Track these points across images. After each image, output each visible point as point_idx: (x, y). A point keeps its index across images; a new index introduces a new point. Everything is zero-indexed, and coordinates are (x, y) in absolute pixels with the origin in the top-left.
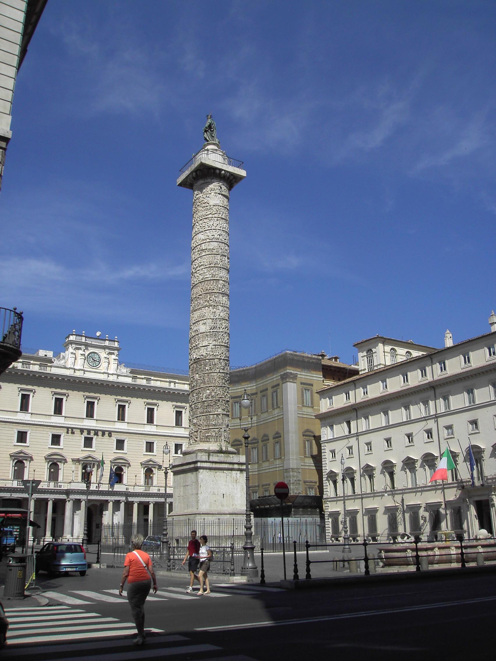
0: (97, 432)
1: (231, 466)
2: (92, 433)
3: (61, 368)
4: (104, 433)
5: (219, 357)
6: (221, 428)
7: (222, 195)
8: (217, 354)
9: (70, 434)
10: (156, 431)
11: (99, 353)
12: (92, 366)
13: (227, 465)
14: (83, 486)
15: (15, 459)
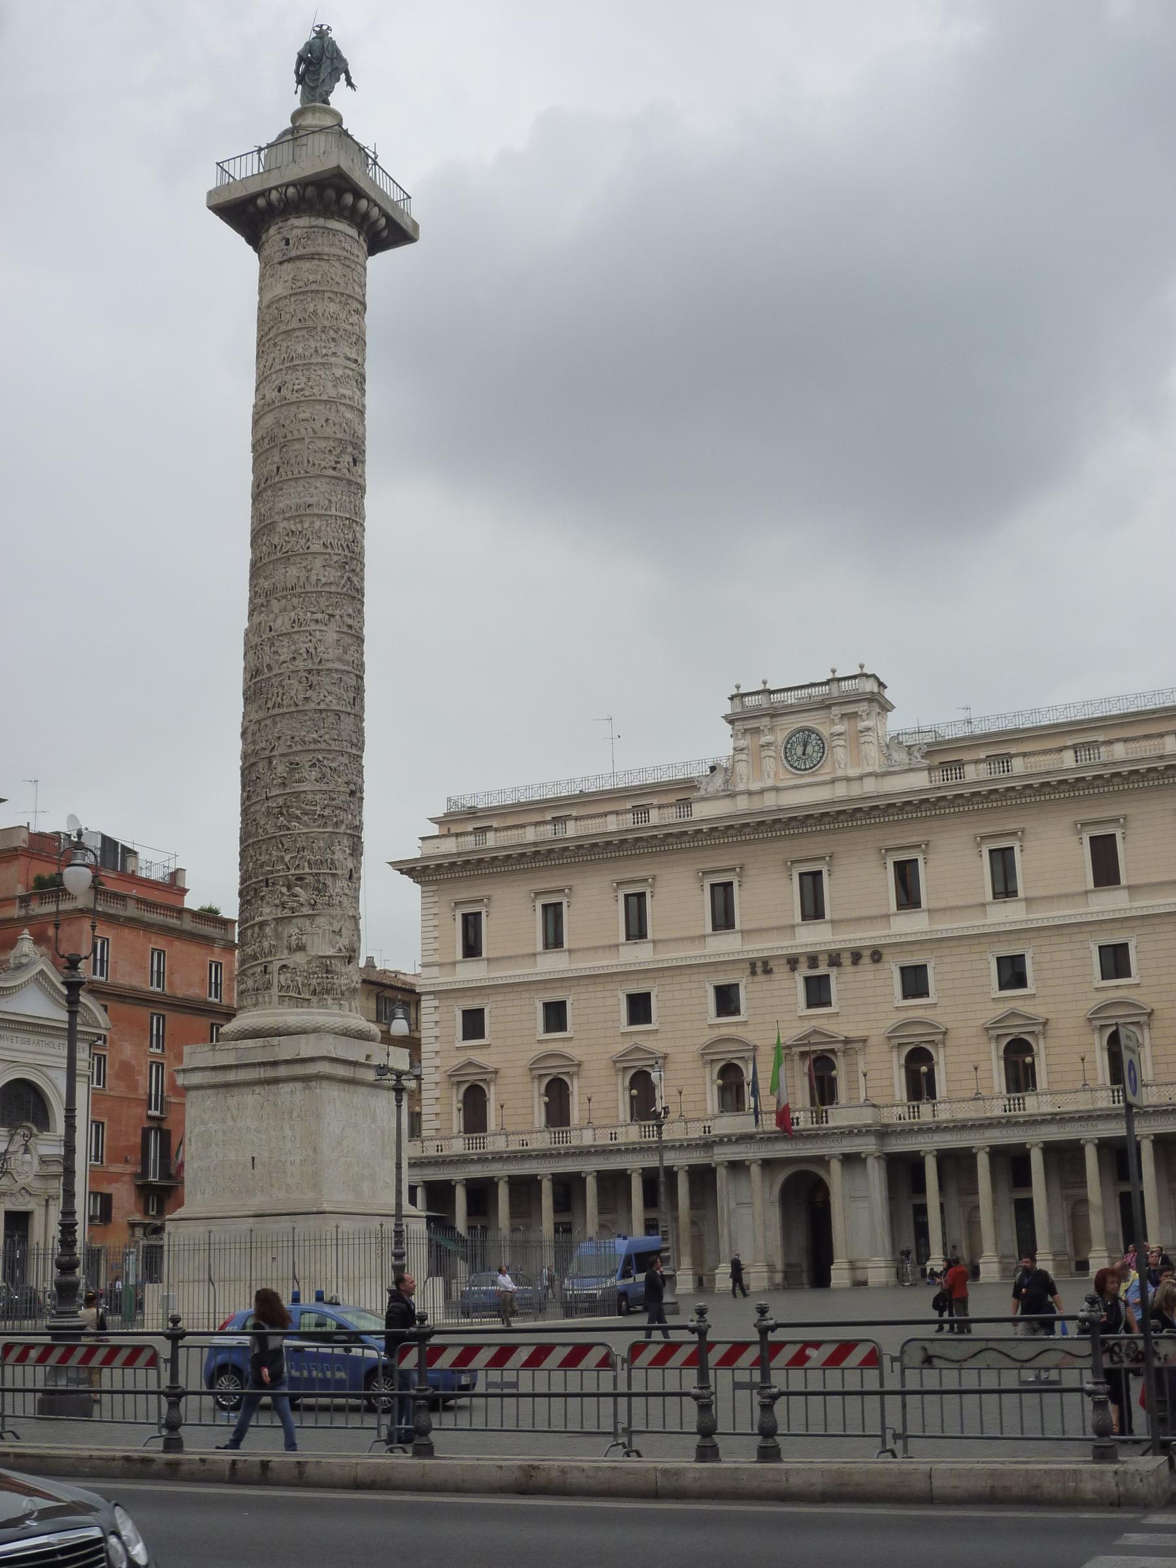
0: (839, 955)
1: (269, 1073)
2: (823, 961)
3: (715, 798)
4: (856, 957)
5: (267, 753)
6: (271, 962)
7: (289, 260)
8: (263, 745)
9: (761, 978)
10: (1024, 917)
11: (816, 727)
12: (800, 770)
13: (258, 1069)
14: (632, 1134)
15: (459, 1083)
